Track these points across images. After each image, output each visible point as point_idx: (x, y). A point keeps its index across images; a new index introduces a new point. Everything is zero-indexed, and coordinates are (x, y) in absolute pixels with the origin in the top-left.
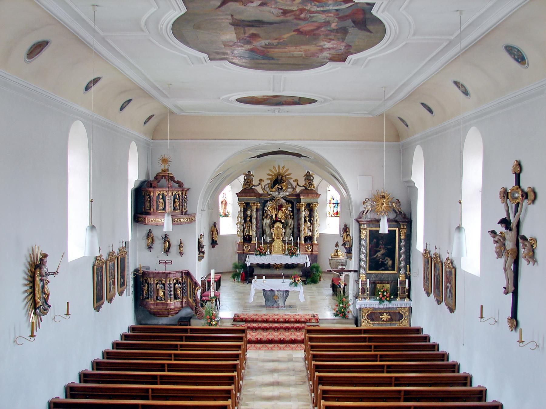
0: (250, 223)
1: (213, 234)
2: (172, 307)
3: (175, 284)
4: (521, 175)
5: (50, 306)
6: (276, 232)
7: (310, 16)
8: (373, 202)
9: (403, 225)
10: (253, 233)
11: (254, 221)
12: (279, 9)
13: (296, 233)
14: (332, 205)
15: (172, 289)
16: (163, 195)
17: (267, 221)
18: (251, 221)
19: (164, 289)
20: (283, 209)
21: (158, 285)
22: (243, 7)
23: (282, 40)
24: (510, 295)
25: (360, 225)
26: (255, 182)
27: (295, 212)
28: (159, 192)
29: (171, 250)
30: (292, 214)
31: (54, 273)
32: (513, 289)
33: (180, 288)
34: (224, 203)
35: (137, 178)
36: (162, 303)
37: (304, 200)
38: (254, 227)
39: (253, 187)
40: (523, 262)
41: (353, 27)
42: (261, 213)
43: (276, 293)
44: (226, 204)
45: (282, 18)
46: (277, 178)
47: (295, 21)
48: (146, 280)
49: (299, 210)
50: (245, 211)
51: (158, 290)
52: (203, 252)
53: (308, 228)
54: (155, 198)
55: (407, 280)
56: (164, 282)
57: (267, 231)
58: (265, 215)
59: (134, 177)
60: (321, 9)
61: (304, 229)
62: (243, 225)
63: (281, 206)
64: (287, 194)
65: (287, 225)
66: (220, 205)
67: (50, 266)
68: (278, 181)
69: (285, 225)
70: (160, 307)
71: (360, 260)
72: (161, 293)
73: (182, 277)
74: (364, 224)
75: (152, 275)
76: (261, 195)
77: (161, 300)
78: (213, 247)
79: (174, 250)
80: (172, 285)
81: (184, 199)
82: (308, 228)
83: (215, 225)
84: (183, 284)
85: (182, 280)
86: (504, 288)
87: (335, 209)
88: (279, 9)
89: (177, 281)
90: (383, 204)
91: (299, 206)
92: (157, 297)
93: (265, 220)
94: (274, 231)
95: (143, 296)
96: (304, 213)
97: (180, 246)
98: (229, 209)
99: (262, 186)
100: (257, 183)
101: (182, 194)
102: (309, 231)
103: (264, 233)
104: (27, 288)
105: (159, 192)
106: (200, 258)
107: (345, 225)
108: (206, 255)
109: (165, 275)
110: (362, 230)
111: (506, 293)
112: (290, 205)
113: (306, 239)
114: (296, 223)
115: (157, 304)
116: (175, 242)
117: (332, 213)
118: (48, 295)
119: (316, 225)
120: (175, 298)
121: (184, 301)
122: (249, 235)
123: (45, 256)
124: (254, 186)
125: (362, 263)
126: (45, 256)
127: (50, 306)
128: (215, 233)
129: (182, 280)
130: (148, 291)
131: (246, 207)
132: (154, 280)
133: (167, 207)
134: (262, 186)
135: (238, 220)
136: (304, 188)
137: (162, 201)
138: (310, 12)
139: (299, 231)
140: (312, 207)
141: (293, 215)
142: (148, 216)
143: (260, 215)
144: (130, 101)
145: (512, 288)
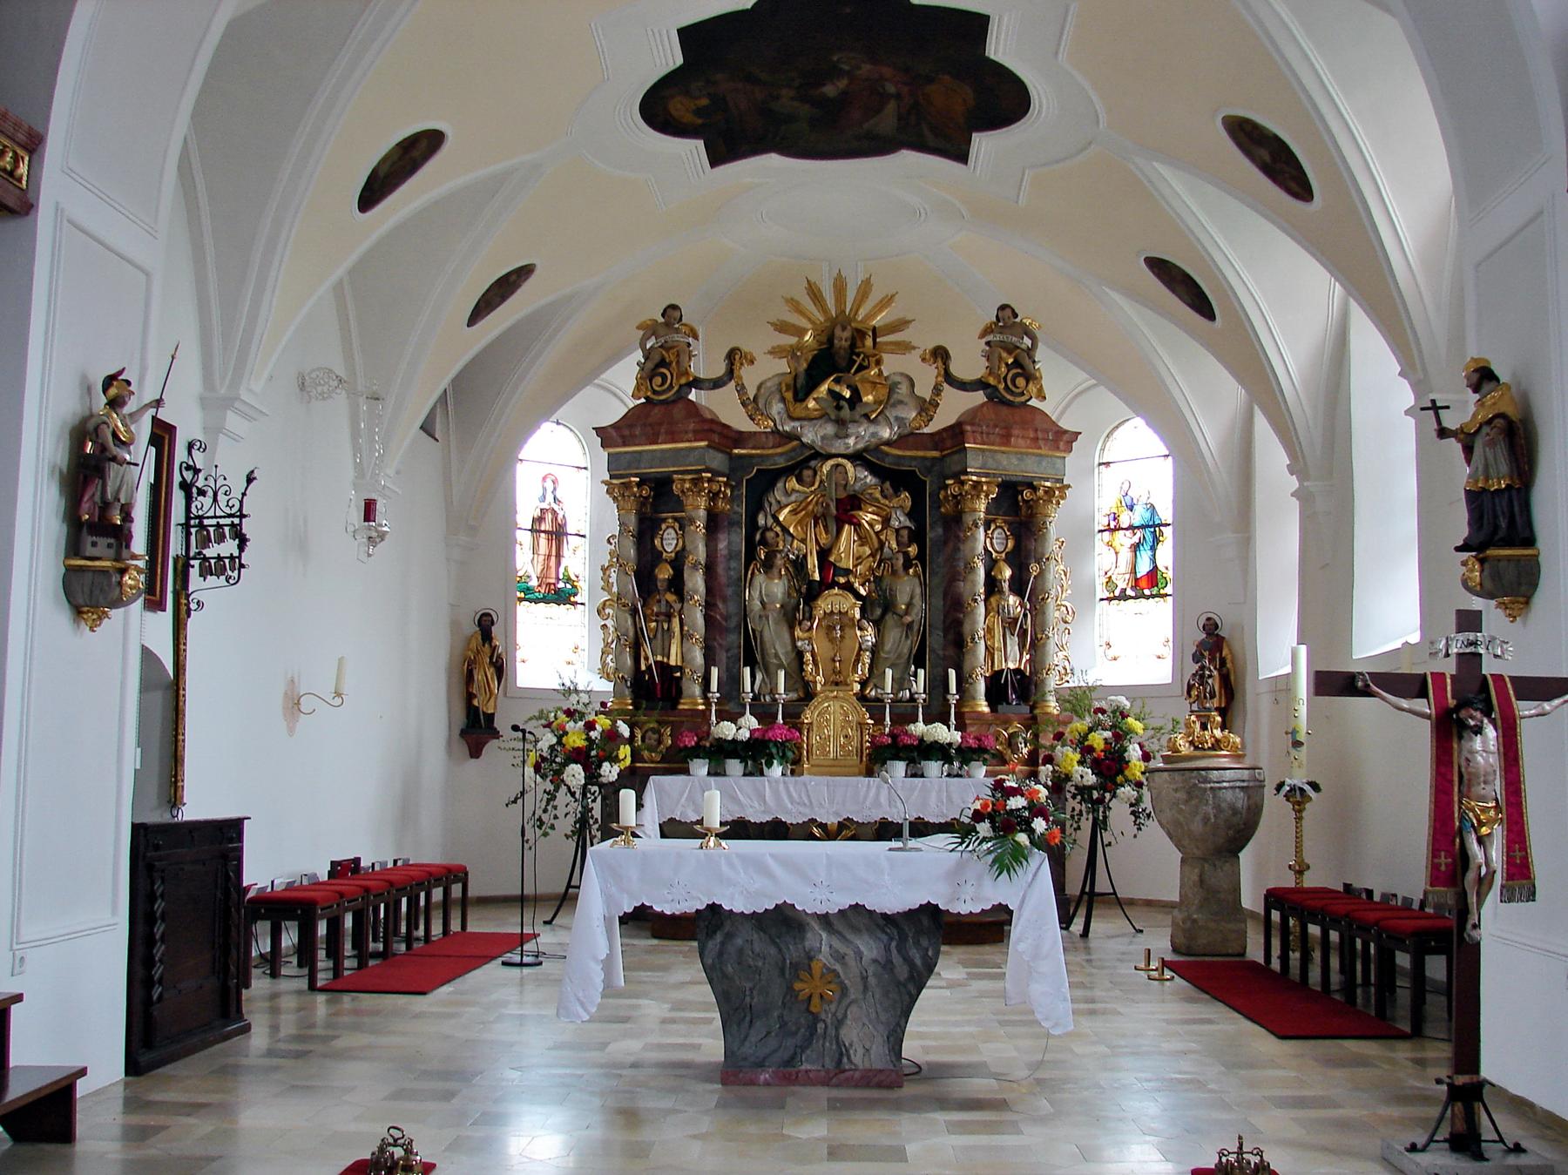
0: (671, 597)
1: (469, 678)
6: (821, 646)
11: (696, 582)
13: (946, 641)
14: (1124, 540)
17: (772, 588)
18: (677, 585)
20: (867, 517)
26: (705, 362)
27: (934, 533)
30: (913, 550)
34: (546, 526)
37: (985, 463)
38: (697, 618)
42: (732, 541)
43: (822, 943)
44: (558, 534)
46: (831, 340)
49: (955, 523)
50: (645, 531)
53: (1011, 624)
57: (776, 640)
58: (758, 550)
61: (989, 630)
62: (634, 612)
63: (847, 508)
64: (886, 433)
65: (888, 606)
66: (524, 537)
68: (836, 357)
69: (879, 607)
76: (740, 438)
78: (475, 752)
82: (1011, 624)
83: (485, 625)
91: (954, 501)
93: (760, 579)
94: (814, 642)
96: (986, 539)
99: (741, 389)
100: (720, 370)
102: (1013, 643)
103: (752, 655)
107: (1211, 627)
112: (905, 498)
113: (997, 689)
114: (938, 602)
117: (1122, 583)
119: (1053, 614)
122: (664, 668)
124: (697, 383)
131: (648, 501)
134: (741, 389)
135: (607, 587)
136: (979, 397)
139: (958, 644)
141: (921, 556)
143: (732, 556)
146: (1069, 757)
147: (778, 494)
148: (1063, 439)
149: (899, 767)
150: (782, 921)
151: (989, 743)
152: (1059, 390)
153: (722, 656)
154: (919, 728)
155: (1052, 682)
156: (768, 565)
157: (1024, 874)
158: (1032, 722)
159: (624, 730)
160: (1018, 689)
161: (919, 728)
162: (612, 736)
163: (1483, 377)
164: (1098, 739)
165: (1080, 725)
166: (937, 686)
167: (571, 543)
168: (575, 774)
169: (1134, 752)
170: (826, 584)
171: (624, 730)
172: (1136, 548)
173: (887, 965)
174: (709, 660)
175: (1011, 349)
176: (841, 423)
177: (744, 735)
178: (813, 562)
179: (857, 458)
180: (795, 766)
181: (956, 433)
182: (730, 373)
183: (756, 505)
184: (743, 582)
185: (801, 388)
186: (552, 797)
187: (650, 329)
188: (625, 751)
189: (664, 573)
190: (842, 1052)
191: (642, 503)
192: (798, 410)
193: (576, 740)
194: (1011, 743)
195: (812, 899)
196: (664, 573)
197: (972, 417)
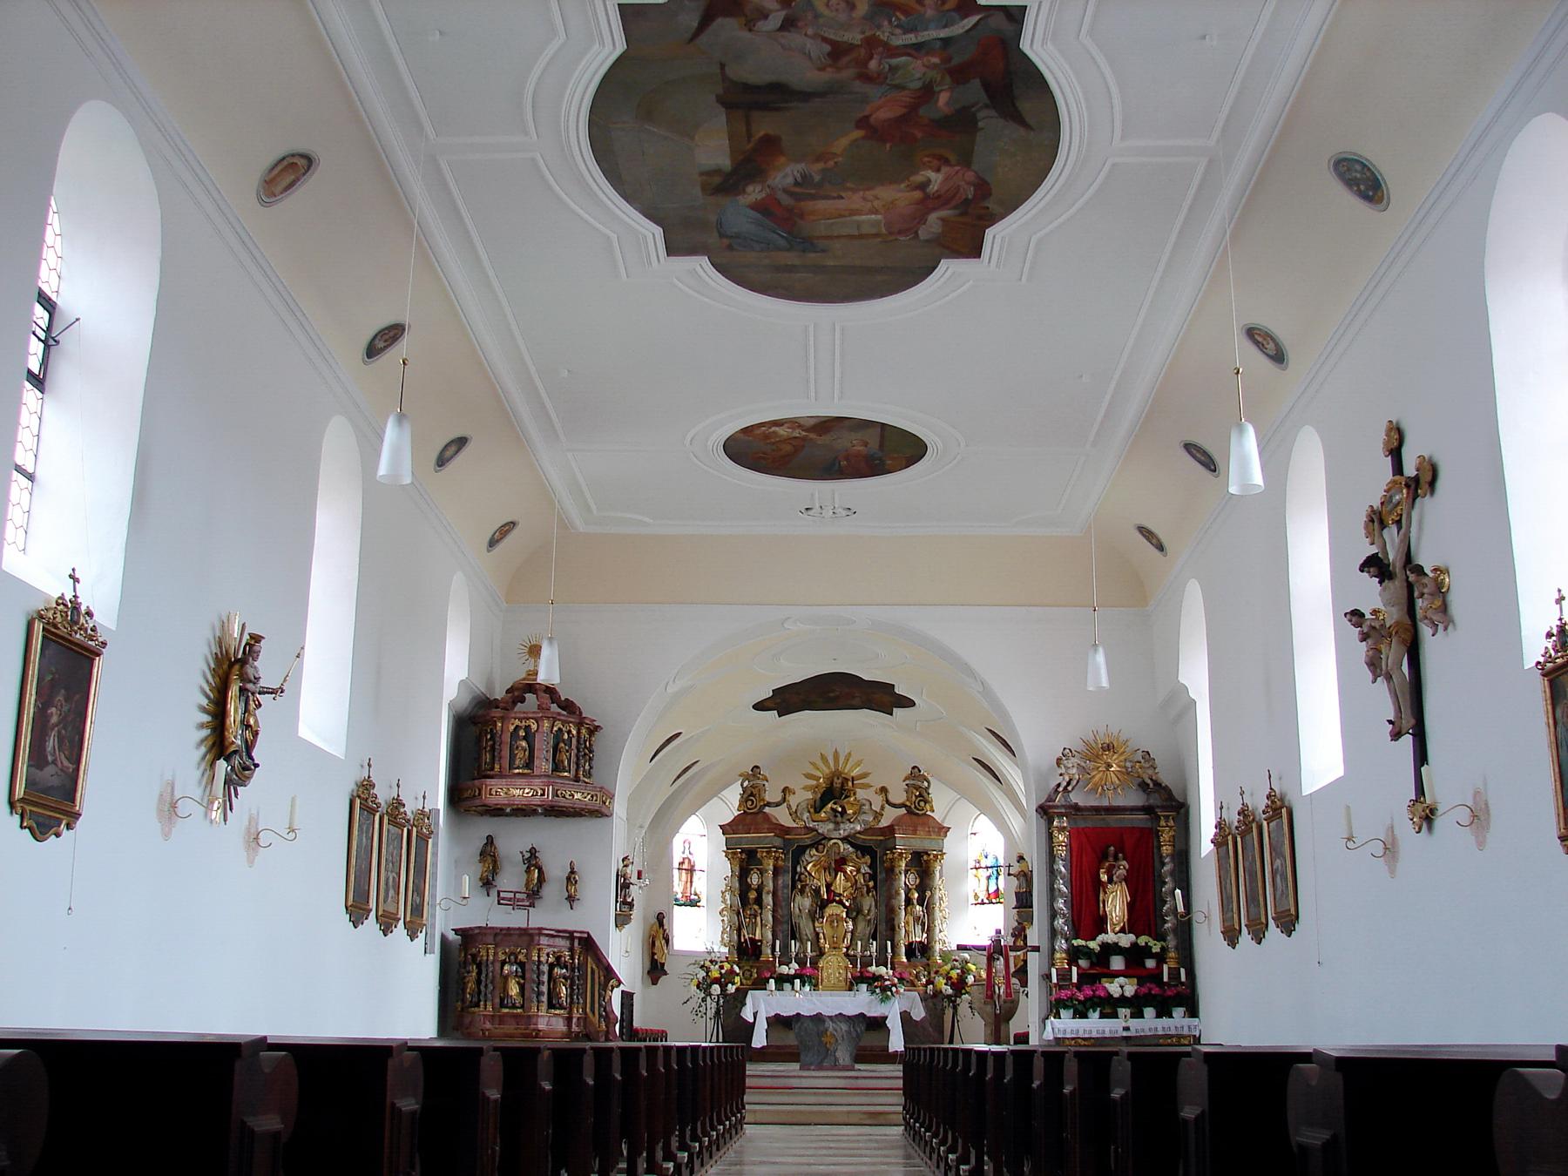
2: (540, 1027)
3: (551, 966)
4: (1404, 450)
5: (257, 766)
6: (827, 930)
7: (891, 68)
8: (1086, 758)
9: (1167, 818)
10: (763, 933)
11: (768, 900)
12: (825, 40)
13: (886, 928)
14: (983, 873)
15: (545, 978)
16: (528, 728)
17: (804, 903)
19: (523, 977)
21: (506, 967)
22: (746, 35)
23: (831, 163)
24: (1407, 740)
25: (1050, 822)
26: (772, 794)
27: (881, 876)
28: (517, 722)
29: (546, 890)
30: (871, 884)
31: (274, 692)
32: (1413, 722)
33: (565, 978)
35: (464, 675)
36: (516, 1016)
37: (904, 843)
39: (767, 810)
40: (1425, 630)
41: (987, 106)
43: (830, 1025)
44: (691, 871)
45: (827, 76)
47: (858, 86)
48: (474, 956)
49: (891, 872)
50: (743, 875)
51: (506, 978)
52: (631, 905)
53: (917, 919)
54: (507, 738)
55: (1183, 971)
56: (521, 957)
57: (806, 927)
58: (798, 883)
59: (456, 671)
60: (911, 38)
61: (907, 923)
62: (738, 913)
63: (840, 864)
65: (859, 911)
66: (676, 872)
67: (266, 669)
68: (834, 792)
69: (854, 912)
70: (509, 1028)
71: (1053, 914)
72: (514, 990)
73: (571, 949)
74: (1061, 815)
75: (490, 939)
76: (788, 830)
77: (514, 1006)
78: (655, 982)
79: (553, 891)
80: (545, 968)
81: (586, 752)
82: (917, 919)
83: (660, 918)
84: (573, 970)
85: (572, 958)
86: (1390, 722)
87: (993, 881)
88: (825, 40)
89: (558, 958)
90: (1110, 766)
91: (892, 860)
92: (502, 1000)
93: (798, 898)
94: (824, 927)
95: (463, 1001)
96: (905, 880)
97: (571, 878)
98: (700, 884)
99: (789, 807)
100: (779, 798)
101: (579, 732)
103: (794, 934)
104: (206, 718)
105: (517, 722)
106: (622, 920)
108: (636, 913)
109: (526, 938)
110: (1056, 833)
111: (1396, 735)
112: (868, 859)
114: (883, 908)
115: (502, 1019)
116: (556, 870)
118: (256, 734)
119: (938, 914)
120: (551, 1006)
121: (576, 1015)
122: (753, 941)
123: (256, 639)
124: (768, 804)
125: (1060, 922)
126: (256, 639)
127: (257, 766)
128: (660, 942)
129: (572, 958)
130: (479, 982)
131: (745, 861)
132: (495, 954)
133: (536, 762)
134: (789, 807)
135: (724, 901)
136: (903, 811)
137: (524, 744)
138: (893, 52)
139: (892, 929)
140: (927, 862)
141: (875, 887)
142: (488, 781)
143: (785, 886)
144: (461, 442)
145: (1408, 721)
146: (941, 982)
147: (807, 856)
148: (943, 831)
149: (864, 987)
150: (818, 1018)
151: (906, 976)
152: (941, 804)
153: (780, 935)
154: (873, 969)
155: (938, 947)
156: (802, 891)
157: (889, 1004)
158: (927, 967)
159: (736, 969)
160: (920, 951)
161: (873, 969)
162: (731, 971)
163: (1021, 858)
164: (954, 974)
165: (948, 967)
166: (882, 949)
167: (697, 875)
168: (716, 989)
169: (970, 979)
170: (829, 901)
171: (736, 969)
172: (989, 878)
173: (849, 1032)
174: (775, 937)
175: (918, 788)
176: (837, 824)
177: (792, 972)
178: (823, 890)
179: (844, 839)
180: (815, 987)
181: (890, 830)
182: (784, 800)
183: (796, 861)
184: (790, 900)
185: (818, 807)
186: (704, 1000)
187: (746, 777)
188: (737, 979)
189: (752, 895)
190: (836, 1060)
191: (742, 861)
192: (816, 817)
193: (715, 974)
194: (917, 976)
195: (827, 1012)
196: (752, 895)
197: (899, 820)
